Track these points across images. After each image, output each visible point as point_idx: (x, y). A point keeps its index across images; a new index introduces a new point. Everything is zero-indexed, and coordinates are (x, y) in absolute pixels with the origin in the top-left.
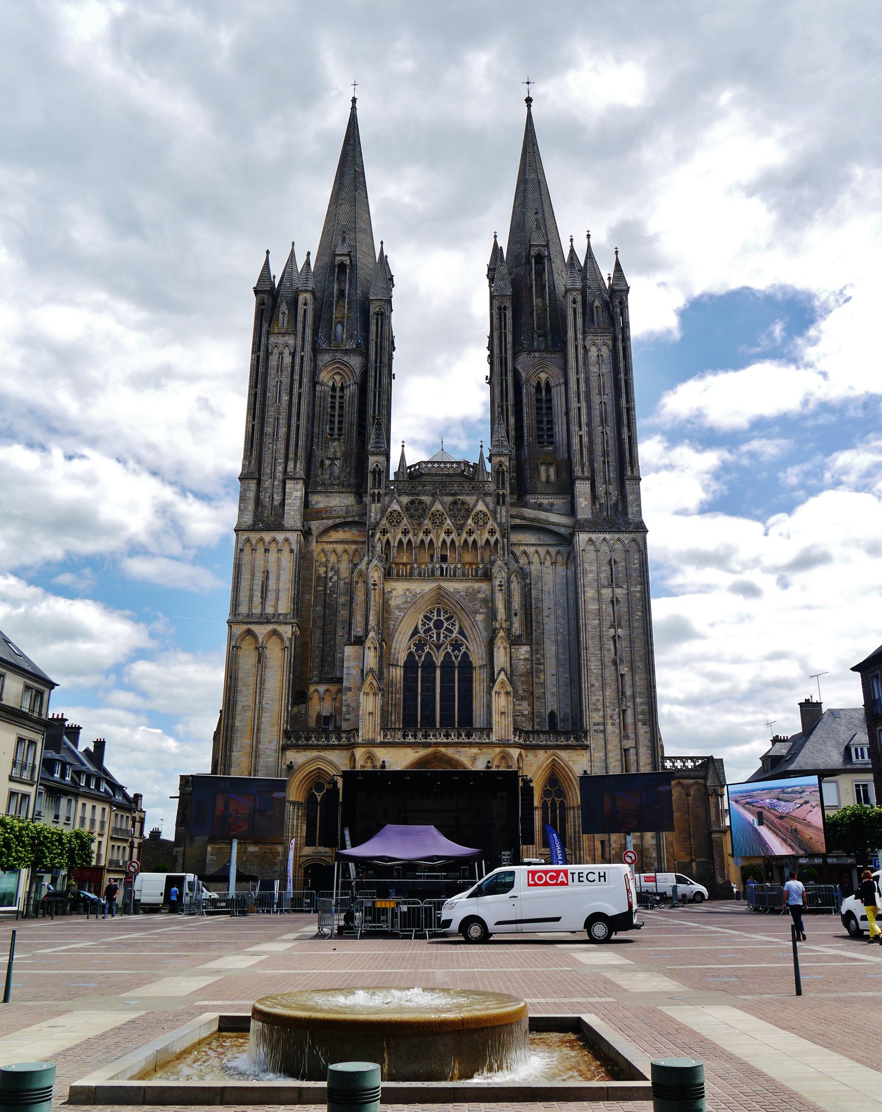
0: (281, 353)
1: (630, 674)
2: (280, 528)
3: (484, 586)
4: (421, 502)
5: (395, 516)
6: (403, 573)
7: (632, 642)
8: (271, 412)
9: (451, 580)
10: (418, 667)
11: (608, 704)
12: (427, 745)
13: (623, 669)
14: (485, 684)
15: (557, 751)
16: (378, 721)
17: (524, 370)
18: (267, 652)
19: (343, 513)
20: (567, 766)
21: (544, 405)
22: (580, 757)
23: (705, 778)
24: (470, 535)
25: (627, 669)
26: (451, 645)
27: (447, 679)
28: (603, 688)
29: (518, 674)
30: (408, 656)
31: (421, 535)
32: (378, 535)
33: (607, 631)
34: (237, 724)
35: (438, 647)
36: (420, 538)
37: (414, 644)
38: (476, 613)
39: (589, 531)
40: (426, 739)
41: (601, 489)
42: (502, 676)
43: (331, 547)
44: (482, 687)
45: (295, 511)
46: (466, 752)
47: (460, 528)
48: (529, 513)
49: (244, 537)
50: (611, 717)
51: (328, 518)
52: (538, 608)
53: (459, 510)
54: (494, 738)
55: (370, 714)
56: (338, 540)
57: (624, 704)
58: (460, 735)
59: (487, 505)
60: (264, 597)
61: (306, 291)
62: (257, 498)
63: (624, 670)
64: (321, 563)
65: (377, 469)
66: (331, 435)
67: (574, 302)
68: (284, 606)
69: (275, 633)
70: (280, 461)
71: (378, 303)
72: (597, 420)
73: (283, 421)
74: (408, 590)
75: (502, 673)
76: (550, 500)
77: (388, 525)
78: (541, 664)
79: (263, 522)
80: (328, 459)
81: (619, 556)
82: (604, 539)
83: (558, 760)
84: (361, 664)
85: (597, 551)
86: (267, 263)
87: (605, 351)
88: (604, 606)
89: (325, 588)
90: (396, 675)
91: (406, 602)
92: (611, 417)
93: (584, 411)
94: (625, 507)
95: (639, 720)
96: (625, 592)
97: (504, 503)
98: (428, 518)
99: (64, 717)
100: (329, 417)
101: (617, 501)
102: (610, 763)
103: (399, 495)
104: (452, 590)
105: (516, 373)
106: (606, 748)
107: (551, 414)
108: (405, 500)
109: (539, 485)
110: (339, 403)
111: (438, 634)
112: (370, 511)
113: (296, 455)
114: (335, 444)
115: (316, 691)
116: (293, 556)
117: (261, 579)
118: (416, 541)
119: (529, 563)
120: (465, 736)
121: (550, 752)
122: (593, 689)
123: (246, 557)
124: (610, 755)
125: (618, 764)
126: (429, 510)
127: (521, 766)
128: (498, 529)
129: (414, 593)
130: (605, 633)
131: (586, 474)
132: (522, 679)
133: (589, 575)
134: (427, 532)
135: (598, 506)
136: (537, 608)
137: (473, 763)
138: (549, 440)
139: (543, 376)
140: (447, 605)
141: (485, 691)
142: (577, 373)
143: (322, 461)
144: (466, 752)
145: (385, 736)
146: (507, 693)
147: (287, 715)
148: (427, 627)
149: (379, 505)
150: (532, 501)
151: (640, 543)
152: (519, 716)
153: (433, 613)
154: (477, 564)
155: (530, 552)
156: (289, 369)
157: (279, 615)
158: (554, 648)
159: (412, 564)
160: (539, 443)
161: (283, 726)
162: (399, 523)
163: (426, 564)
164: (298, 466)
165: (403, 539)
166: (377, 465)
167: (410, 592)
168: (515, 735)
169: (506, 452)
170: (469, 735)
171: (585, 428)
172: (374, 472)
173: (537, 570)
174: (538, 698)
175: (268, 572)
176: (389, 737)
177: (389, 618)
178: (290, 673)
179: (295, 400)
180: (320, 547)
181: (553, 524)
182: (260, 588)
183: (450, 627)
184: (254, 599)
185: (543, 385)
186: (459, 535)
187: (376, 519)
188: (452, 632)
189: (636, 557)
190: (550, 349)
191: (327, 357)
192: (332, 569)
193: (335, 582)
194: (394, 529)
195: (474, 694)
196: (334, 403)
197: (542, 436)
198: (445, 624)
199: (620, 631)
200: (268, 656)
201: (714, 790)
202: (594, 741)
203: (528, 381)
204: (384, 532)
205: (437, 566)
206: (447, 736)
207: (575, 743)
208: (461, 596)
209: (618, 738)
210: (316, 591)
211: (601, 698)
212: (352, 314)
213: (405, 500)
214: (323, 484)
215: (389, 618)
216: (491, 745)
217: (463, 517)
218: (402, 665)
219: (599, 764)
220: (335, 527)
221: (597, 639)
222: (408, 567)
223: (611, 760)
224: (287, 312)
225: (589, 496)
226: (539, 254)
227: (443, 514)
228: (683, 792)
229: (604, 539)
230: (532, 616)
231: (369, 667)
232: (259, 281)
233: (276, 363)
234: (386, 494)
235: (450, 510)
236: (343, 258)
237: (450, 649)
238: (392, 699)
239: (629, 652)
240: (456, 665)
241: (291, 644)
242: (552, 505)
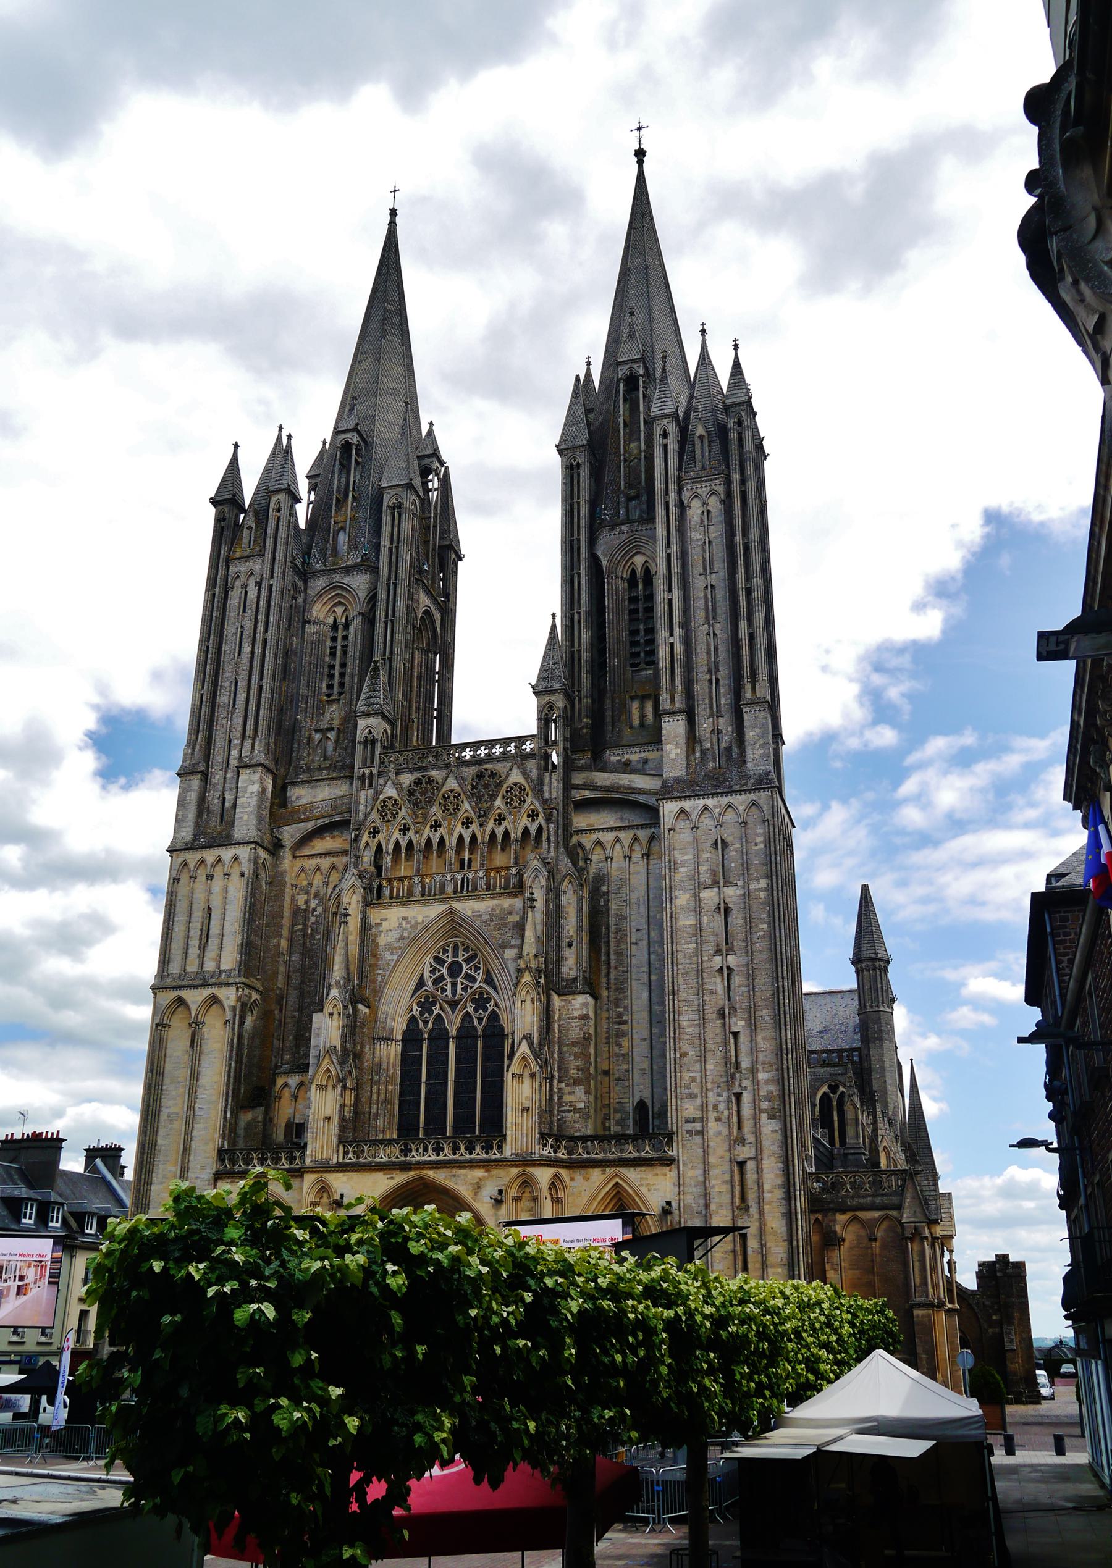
0: (244, 586)
1: (748, 1032)
2: (227, 841)
3: (517, 902)
4: (430, 781)
6: (398, 894)
7: (751, 976)
8: (227, 673)
9: (468, 899)
11: (709, 1086)
12: (405, 1167)
13: (736, 1024)
15: (622, 1170)
16: (335, 1130)
17: (605, 555)
18: (205, 1029)
19: (329, 811)
20: (638, 1195)
21: (641, 606)
22: (661, 1178)
23: (899, 1208)
24: (500, 824)
25: (743, 1023)
26: (473, 1001)
27: (465, 1056)
28: (702, 1058)
29: (570, 1042)
30: (408, 1023)
31: (427, 831)
32: (365, 838)
33: (710, 960)
34: (159, 1142)
35: (453, 1005)
36: (425, 836)
37: (418, 1003)
38: (505, 947)
39: (680, 798)
40: (406, 1156)
41: (705, 726)
42: (524, 1048)
43: (313, 862)
45: (249, 813)
46: (465, 1175)
47: (483, 815)
48: (603, 778)
49: (180, 860)
50: (715, 1107)
51: (306, 820)
52: (620, 930)
53: (486, 786)
54: (508, 1152)
55: (329, 1118)
56: (323, 851)
57: (737, 1083)
58: (455, 1149)
59: (525, 774)
60: (203, 948)
61: (279, 491)
62: (202, 799)
63: (738, 1024)
64: (301, 889)
66: (329, 695)
67: (665, 435)
68: (230, 959)
69: (214, 1000)
70: (236, 742)
71: (393, 492)
72: (700, 615)
73: (242, 685)
74: (405, 918)
75: (524, 1042)
76: (643, 755)
77: (378, 821)
78: (625, 1022)
79: (205, 834)
80: (317, 731)
81: (730, 833)
82: (706, 808)
83: (624, 1185)
85: (694, 828)
86: (234, 460)
87: (714, 504)
88: (705, 919)
89: (305, 925)
90: (388, 1055)
91: (402, 938)
92: (723, 607)
93: (676, 604)
94: (742, 751)
95: (761, 1111)
96: (739, 892)
98: (437, 803)
99: (60, 1136)
100: (326, 670)
101: (731, 743)
102: (713, 1187)
104: (469, 914)
105: (594, 560)
106: (705, 1161)
107: (653, 618)
108: (407, 779)
109: (627, 731)
110: (343, 646)
111: (454, 985)
113: (256, 730)
114: (334, 707)
115: (286, 1085)
116: (244, 881)
117: (200, 920)
118: (419, 842)
119: (607, 858)
120: (466, 1149)
121: (609, 1171)
122: (685, 1060)
123: (183, 889)
124: (714, 1172)
125: (726, 1188)
127: (561, 1195)
128: (540, 810)
129: (413, 923)
130: (705, 965)
131: (677, 705)
132: (576, 1050)
133: (681, 870)
134: (436, 826)
135: (698, 754)
136: (619, 930)
137: (476, 1194)
138: (648, 659)
139: (639, 560)
140: (467, 937)
142: (668, 545)
143: (309, 738)
144: (465, 1175)
145: (346, 1153)
146: (533, 1076)
147: (224, 1126)
148: (438, 974)
149: (371, 791)
150: (614, 759)
151: (765, 808)
152: (571, 1111)
153: (448, 951)
154: (507, 868)
155: (608, 841)
156: (254, 606)
157: (221, 972)
158: (645, 995)
159: (411, 878)
160: (632, 665)
161: (218, 1142)
162: (394, 816)
163: (432, 876)
164: (256, 747)
165: (401, 840)
167: (408, 923)
169: (558, 686)
170: (470, 1149)
171: (677, 631)
172: (365, 742)
173: (619, 869)
174: (619, 1079)
175: (209, 909)
176: (351, 1155)
177: (377, 966)
178: (230, 1059)
179: (258, 651)
180: (299, 863)
181: (641, 792)
182: (199, 933)
183: (472, 973)
184: (190, 951)
185: (639, 574)
186: (481, 825)
188: (473, 980)
189: (760, 831)
190: (645, 516)
191: (320, 583)
192: (316, 896)
193: (320, 916)
194: (388, 826)
196: (335, 648)
197: (637, 654)
198: (465, 969)
199: (732, 960)
200: (206, 1036)
201: (916, 1228)
202: (684, 1150)
203: (611, 571)
204: (375, 832)
205: (449, 877)
206: (438, 1150)
207: (651, 1154)
208: (482, 922)
209: (728, 1143)
210: (292, 931)
211: (697, 1075)
212: (361, 514)
213: (407, 779)
214: (308, 769)
215: (376, 966)
216: (503, 1163)
218: (400, 1038)
219: (694, 1190)
220: (318, 832)
221: (693, 975)
222: (406, 882)
223: (713, 1182)
224: (253, 526)
225: (682, 740)
226: (631, 374)
227: (459, 795)
228: (863, 1233)
229: (706, 808)
230: (608, 946)
231: (328, 1045)
232: (219, 488)
233: (237, 600)
234: (380, 774)
236: (348, 435)
237: (470, 1007)
238: (379, 1095)
239: (746, 994)
240: (480, 1033)
241: (235, 1015)
242: (646, 761)
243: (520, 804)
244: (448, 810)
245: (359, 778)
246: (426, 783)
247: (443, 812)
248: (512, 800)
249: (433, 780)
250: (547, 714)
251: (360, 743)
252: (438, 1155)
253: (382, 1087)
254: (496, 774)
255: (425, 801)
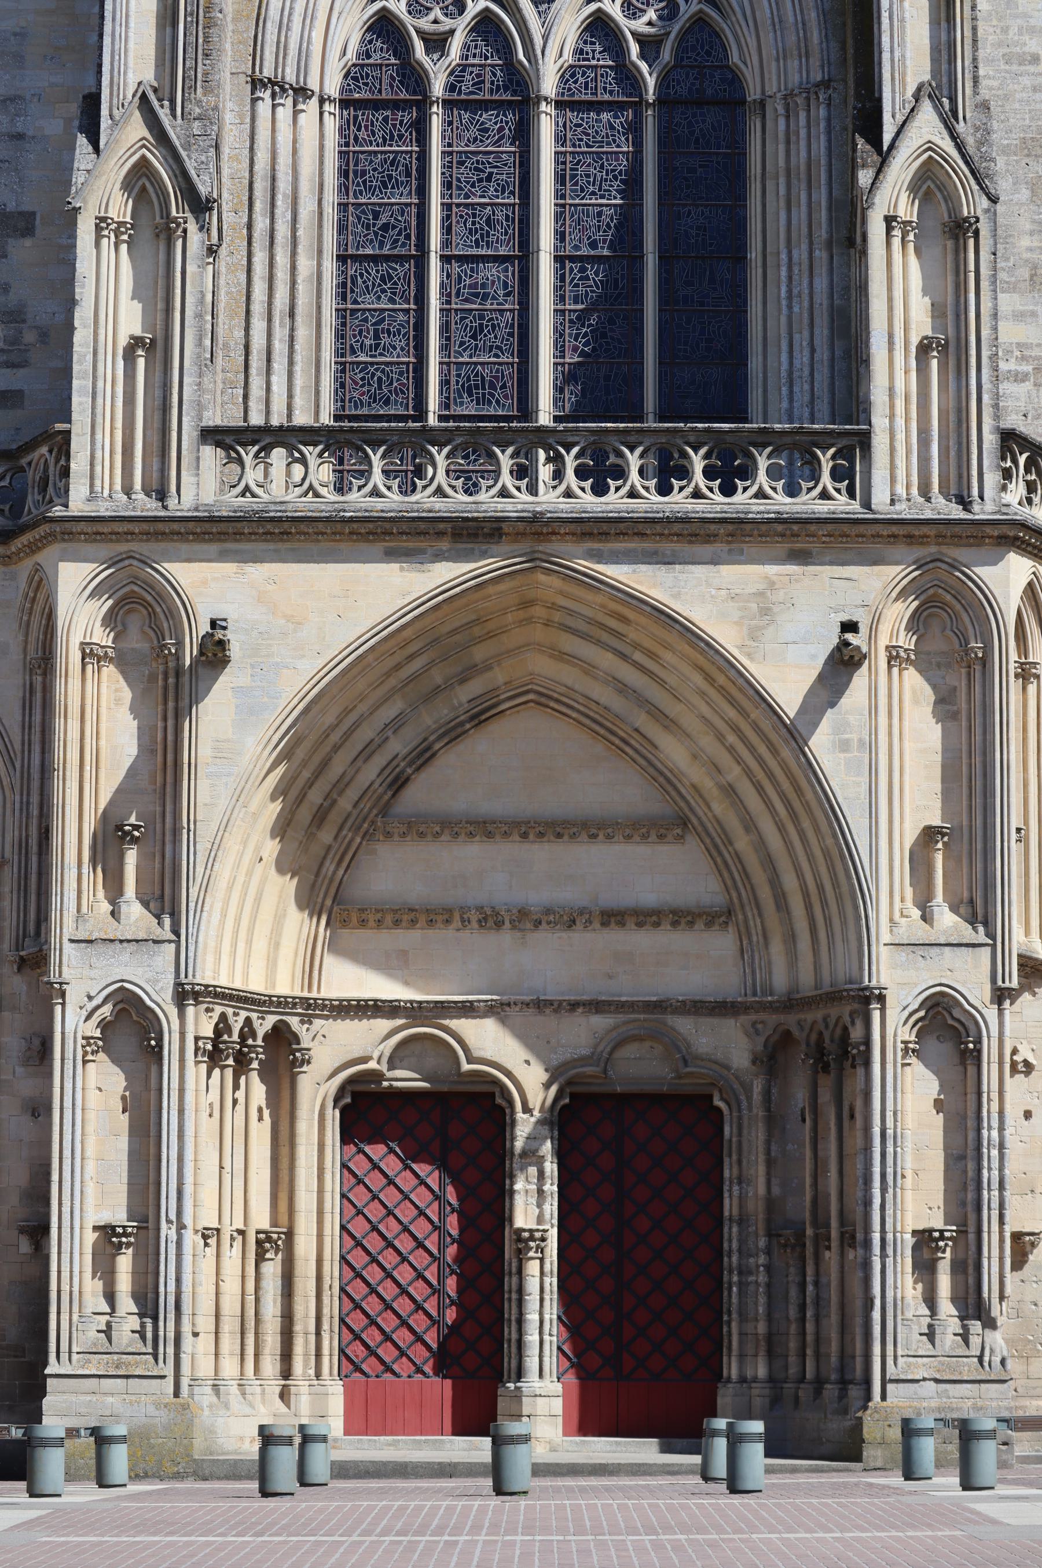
10: (423, 103)
14: (822, 196)
44: (801, 214)
84: (91, 81)
120: (709, 473)
141: (822, 233)
168: (1007, 474)
195: (754, 254)
218: (333, 87)
252: (600, 490)
253: (282, 259)
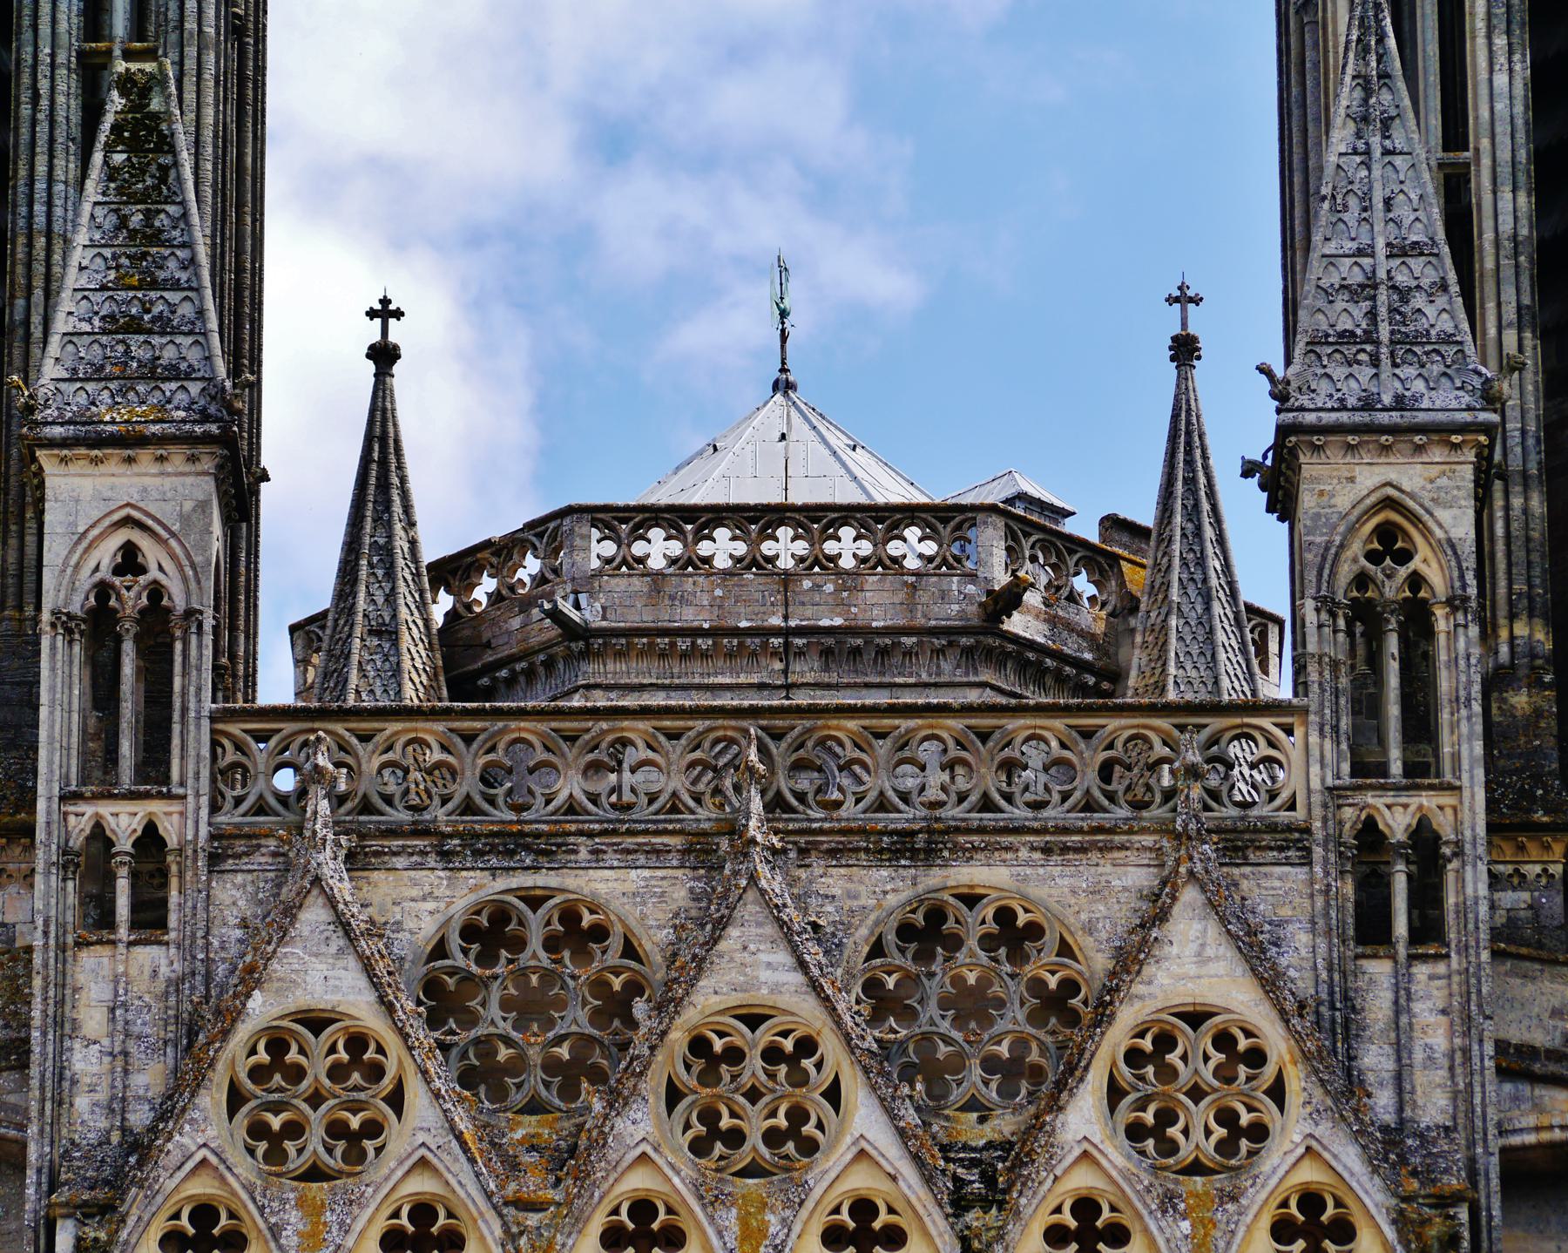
5: (317, 1070)
65: (132, 599)
77: (245, 1168)
97: (1427, 930)
98: (653, 1086)
103: (356, 861)
112: (63, 1026)
126: (668, 1005)
166: (129, 550)
187: (118, 1105)
194: (312, 1210)
217: (1009, 1071)
227: (807, 1046)
235: (881, 1002)
243: (1226, 1147)
244: (735, 1138)
245: (68, 862)
246: (551, 944)
247: (699, 1148)
248: (1167, 1117)
249: (600, 933)
250: (1362, 580)
251: (65, 622)
254: (1034, 931)
255: (552, 1066)
